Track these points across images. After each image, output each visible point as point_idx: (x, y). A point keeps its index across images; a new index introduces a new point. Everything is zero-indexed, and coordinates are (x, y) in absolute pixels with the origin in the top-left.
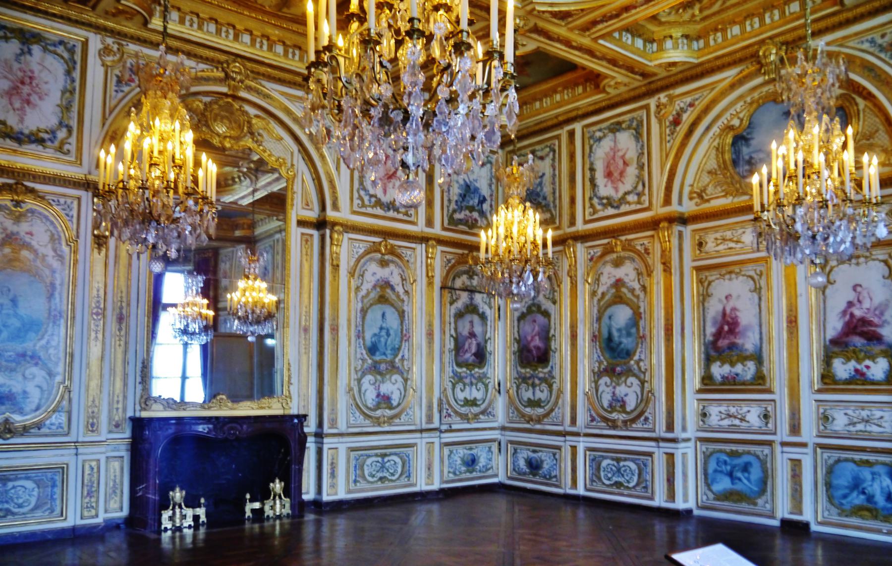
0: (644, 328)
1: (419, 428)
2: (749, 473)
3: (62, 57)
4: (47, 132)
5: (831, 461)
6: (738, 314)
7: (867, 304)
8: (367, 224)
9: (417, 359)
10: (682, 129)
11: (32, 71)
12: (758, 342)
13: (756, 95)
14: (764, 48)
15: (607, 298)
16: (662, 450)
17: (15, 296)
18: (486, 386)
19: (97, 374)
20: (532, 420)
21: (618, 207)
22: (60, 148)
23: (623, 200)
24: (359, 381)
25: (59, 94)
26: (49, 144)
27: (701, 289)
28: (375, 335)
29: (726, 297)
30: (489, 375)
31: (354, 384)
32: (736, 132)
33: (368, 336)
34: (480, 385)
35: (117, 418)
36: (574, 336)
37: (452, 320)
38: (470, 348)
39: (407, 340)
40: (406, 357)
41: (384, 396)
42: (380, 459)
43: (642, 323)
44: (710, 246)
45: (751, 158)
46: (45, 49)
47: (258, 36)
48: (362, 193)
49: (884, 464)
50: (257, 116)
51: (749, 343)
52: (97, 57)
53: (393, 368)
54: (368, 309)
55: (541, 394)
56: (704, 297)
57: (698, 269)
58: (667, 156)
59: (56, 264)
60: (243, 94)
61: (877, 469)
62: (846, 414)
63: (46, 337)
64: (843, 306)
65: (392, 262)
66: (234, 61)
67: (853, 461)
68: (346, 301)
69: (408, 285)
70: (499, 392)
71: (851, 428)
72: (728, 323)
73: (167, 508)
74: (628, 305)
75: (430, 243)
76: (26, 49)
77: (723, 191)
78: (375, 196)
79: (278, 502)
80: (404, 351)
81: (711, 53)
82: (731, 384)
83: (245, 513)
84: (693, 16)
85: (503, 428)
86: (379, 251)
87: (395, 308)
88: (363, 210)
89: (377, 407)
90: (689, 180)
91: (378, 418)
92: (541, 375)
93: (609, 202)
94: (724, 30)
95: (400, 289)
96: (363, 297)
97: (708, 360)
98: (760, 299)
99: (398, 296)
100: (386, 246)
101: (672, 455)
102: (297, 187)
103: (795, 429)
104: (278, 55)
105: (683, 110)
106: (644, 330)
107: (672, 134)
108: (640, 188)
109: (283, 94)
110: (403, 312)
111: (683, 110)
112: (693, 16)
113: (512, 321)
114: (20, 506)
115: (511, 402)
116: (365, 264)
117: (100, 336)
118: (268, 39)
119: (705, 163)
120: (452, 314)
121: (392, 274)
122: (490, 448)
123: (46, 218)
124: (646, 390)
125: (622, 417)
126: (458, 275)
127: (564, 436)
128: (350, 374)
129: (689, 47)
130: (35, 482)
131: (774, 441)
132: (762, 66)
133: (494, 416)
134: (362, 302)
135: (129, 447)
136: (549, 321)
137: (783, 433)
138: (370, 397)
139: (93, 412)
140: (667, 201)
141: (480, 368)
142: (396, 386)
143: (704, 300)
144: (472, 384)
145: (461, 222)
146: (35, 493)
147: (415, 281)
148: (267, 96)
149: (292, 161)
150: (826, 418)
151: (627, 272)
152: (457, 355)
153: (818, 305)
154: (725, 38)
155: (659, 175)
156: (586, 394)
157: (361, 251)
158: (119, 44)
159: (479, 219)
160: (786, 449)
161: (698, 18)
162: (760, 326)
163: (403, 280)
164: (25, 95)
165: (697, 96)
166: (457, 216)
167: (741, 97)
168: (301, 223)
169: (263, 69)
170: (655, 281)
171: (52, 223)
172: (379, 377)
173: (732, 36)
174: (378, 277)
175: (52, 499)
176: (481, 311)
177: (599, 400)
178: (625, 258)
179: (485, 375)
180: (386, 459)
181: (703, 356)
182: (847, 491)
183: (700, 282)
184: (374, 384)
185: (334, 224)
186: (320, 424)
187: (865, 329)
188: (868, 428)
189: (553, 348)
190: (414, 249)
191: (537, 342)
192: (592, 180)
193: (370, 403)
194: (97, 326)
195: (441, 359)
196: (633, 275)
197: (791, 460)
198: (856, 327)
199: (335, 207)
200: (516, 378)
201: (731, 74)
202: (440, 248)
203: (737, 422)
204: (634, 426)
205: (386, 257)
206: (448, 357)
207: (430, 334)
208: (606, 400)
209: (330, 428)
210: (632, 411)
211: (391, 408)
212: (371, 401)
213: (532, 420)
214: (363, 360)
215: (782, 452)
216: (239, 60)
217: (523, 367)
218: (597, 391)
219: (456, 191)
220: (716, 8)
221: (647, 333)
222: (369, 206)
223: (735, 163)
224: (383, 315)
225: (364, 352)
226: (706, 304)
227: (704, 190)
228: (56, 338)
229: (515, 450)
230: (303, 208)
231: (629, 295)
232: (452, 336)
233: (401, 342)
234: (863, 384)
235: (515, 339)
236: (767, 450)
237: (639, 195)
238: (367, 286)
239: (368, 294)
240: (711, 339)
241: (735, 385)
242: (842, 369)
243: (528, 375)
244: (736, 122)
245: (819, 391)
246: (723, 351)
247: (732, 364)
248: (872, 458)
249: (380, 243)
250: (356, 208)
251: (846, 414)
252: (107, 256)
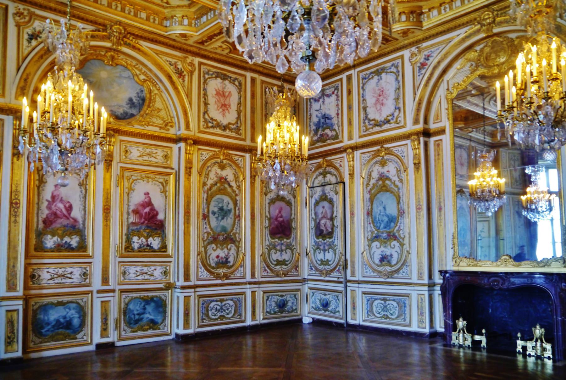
3: (393, 72)
4: (390, 116)
11: (383, 88)
17: (385, 205)
22: (396, 121)
25: (394, 92)
46: (387, 73)
60: (496, 30)
63: (398, 225)
73: (455, 331)
76: (379, 78)
79: (461, 335)
83: (516, 347)
114: (392, 315)
123: (394, 161)
130: (398, 303)
146: (397, 309)
158: (417, 48)
164: (381, 102)
175: (405, 314)
228: (402, 225)
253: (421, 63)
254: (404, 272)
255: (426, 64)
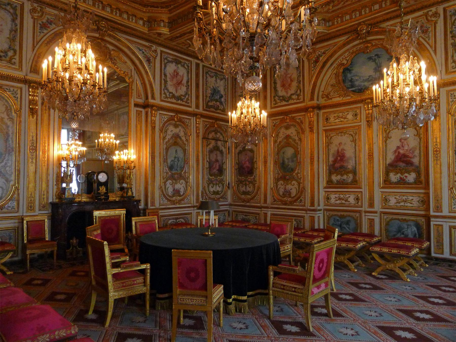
0: (300, 158)
1: (193, 205)
2: (349, 225)
3: (10, 12)
5: (388, 220)
6: (345, 152)
7: (406, 148)
8: (168, 106)
9: (191, 172)
10: (320, 64)
12: (354, 165)
13: (355, 49)
14: (360, 27)
15: (282, 144)
16: (308, 215)
18: (223, 185)
19: (33, 180)
20: (245, 201)
21: (288, 101)
22: (10, 61)
23: (290, 98)
24: (165, 183)
26: (4, 58)
27: (327, 140)
28: (172, 161)
29: (339, 144)
30: (224, 180)
31: (162, 185)
32: (345, 67)
33: (169, 161)
34: (220, 185)
35: (43, 203)
36: (265, 162)
37: (208, 154)
38: (216, 167)
39: (187, 163)
40: (187, 171)
41: (176, 190)
42: (175, 221)
43: (299, 156)
44: (332, 119)
45: (352, 79)
47: (114, 9)
48: (166, 91)
49: (413, 221)
50: (113, 50)
51: (350, 165)
52: (29, 13)
53: (181, 177)
54: (169, 148)
55: (249, 189)
56: (328, 144)
57: (326, 131)
58: (312, 77)
59: (9, 123)
61: (409, 223)
62: (395, 198)
63: (5, 161)
64: (395, 148)
65: (180, 125)
66: (102, 21)
67: (399, 219)
68: (158, 145)
69: (188, 137)
70: (229, 188)
71: (398, 205)
72: (340, 156)
74: (292, 147)
75: (198, 116)
77: (338, 94)
78: (172, 93)
80: (186, 168)
81: (335, 28)
82: (342, 184)
84: (329, 9)
85: (230, 205)
86: (174, 120)
87: (181, 147)
88: (166, 99)
89: (173, 195)
90: (322, 89)
91: (174, 201)
92: (249, 180)
93: (283, 99)
94: (342, 18)
95: (184, 138)
96: (166, 142)
97: (330, 173)
98: (355, 145)
99: (183, 142)
100: (177, 117)
101: (314, 217)
102: (134, 87)
103: (371, 205)
104: (125, 19)
105: (320, 56)
106: (300, 159)
107: (315, 67)
108: (299, 92)
109: (127, 39)
110: (186, 149)
111: (320, 56)
112: (329, 9)
113: (235, 154)
115: (234, 194)
116: (167, 126)
117: (34, 161)
118: (120, 10)
119: (330, 81)
120: (208, 151)
121: (180, 131)
122: (225, 214)
124: (301, 187)
125: (289, 199)
126: (211, 132)
127: (261, 208)
128: (160, 180)
129: (325, 25)
131: (361, 211)
132: (359, 35)
133: (226, 199)
134: (166, 144)
135: (50, 218)
136: (254, 155)
137: (365, 207)
138: (170, 191)
139: (31, 200)
140: (312, 99)
141: (220, 176)
142: (182, 185)
143: (328, 145)
144: (216, 184)
145: (211, 107)
147: (190, 135)
148: (119, 40)
149: (131, 74)
150: (386, 200)
151: (292, 132)
152: (210, 170)
153: (383, 148)
154: (342, 21)
155: (308, 86)
156: (272, 189)
157: (166, 120)
158: (41, 7)
159: (220, 105)
160: (367, 214)
161: (330, 11)
162: (355, 157)
163: (185, 134)
165: (327, 49)
166: (210, 104)
167: (348, 50)
168: (136, 105)
169: (116, 26)
170: (306, 136)
171: (6, 101)
172: (174, 181)
173: (346, 20)
174: (173, 132)
176: (221, 149)
177: (278, 190)
178: (291, 125)
179: (222, 179)
180: (178, 221)
181: (327, 171)
182: (395, 233)
183: (327, 137)
184: (172, 184)
185: (152, 106)
186: (146, 204)
187: (405, 159)
188: (406, 205)
189: (255, 167)
190: (190, 119)
191: (248, 164)
192: (275, 88)
193: (170, 194)
194: (33, 155)
195: (203, 173)
196: (295, 133)
197: (369, 219)
198: (401, 158)
199: (153, 98)
200: (237, 181)
201: (343, 38)
202: (202, 119)
203: (344, 202)
204: (295, 203)
205: (177, 123)
206: (206, 171)
207: (198, 161)
208: (281, 191)
209: (151, 206)
210: (294, 197)
211: (180, 196)
212: (170, 193)
213: (245, 201)
214: (167, 173)
215: (365, 216)
216: (104, 20)
217: (240, 176)
218: (277, 187)
219: (209, 91)
220: (340, 6)
221: (302, 160)
222: (169, 98)
223: (344, 81)
224: (176, 151)
225: (167, 169)
226: (329, 147)
227: (329, 94)
228: (10, 162)
229: (237, 215)
230: (137, 98)
231: (293, 143)
232: (207, 161)
233: (184, 164)
234: (404, 184)
235: (236, 163)
236: (358, 215)
237: (298, 95)
238: (168, 137)
239: (169, 141)
240: (332, 163)
241: (343, 184)
242: (394, 177)
243: (243, 180)
244: (345, 62)
245: (383, 188)
246: (338, 169)
247: (342, 175)
248: (407, 218)
249: (175, 116)
250: (163, 99)
251: (395, 198)
252: (37, 119)
253: (43, 22)
254: (9, 207)
255: (49, 27)
